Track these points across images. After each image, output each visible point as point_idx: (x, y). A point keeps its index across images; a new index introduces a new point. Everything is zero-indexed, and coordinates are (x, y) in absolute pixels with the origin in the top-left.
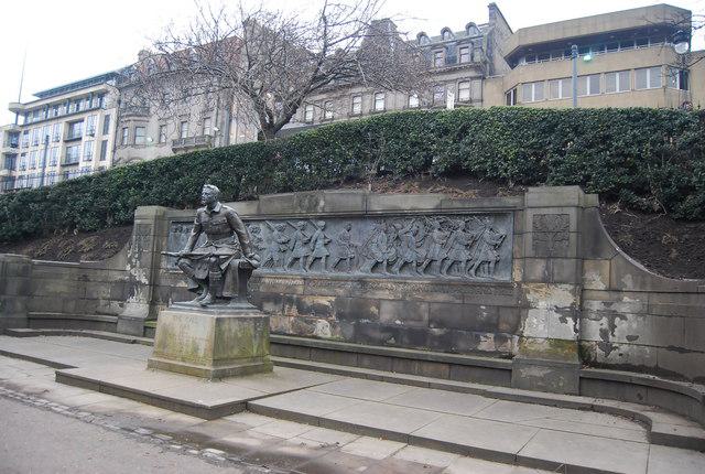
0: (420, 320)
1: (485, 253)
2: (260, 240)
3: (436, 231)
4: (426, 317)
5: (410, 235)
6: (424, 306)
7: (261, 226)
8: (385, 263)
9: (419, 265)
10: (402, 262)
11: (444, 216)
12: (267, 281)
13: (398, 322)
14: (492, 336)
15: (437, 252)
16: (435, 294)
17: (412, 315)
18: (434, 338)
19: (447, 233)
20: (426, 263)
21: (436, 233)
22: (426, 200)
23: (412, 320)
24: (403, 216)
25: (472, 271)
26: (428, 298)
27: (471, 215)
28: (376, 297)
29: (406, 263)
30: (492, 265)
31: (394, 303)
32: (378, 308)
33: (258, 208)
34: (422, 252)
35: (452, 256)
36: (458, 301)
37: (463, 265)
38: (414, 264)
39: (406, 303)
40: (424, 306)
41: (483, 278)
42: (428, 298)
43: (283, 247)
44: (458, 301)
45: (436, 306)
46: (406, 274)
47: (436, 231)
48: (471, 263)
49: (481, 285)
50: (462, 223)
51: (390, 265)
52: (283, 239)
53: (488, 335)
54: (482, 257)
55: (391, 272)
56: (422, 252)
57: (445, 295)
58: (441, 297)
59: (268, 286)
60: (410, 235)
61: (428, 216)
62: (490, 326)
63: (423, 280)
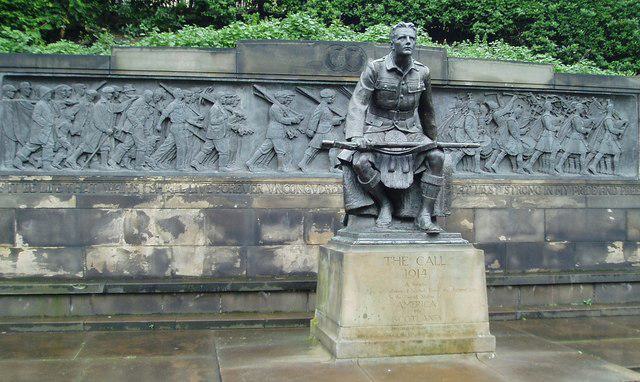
0: (533, 232)
1: (606, 144)
2: (241, 118)
3: (547, 113)
4: (541, 228)
5: (513, 118)
6: (537, 215)
7: (244, 97)
8: (478, 156)
9: (526, 158)
10: (501, 156)
11: (560, 94)
12: (264, 188)
13: (503, 238)
14: (619, 244)
15: (550, 142)
16: (550, 197)
17: (523, 227)
18: (552, 254)
19: (561, 117)
20: (536, 155)
21: (548, 118)
22: (537, 72)
23: (522, 233)
24: (500, 91)
25: (593, 167)
26: (543, 203)
27: (588, 95)
28: (471, 205)
29: (507, 156)
30: (616, 159)
31: (495, 212)
32: (473, 219)
33: (239, 63)
34: (530, 142)
35: (568, 148)
36: (580, 205)
37: (582, 159)
38: (520, 158)
39: (515, 211)
40: (537, 215)
41: (606, 175)
42: (543, 203)
43: (292, 131)
44: (580, 205)
45: (553, 214)
46: (504, 171)
47: (547, 113)
48: (590, 156)
49: (607, 184)
50: (579, 105)
51: (483, 158)
52: (292, 118)
53: (617, 244)
54: (604, 149)
55: (485, 169)
56: (530, 142)
57: (565, 197)
58: (559, 201)
59: (270, 198)
60: (513, 118)
61: (537, 92)
62: (619, 233)
63: (538, 179)
